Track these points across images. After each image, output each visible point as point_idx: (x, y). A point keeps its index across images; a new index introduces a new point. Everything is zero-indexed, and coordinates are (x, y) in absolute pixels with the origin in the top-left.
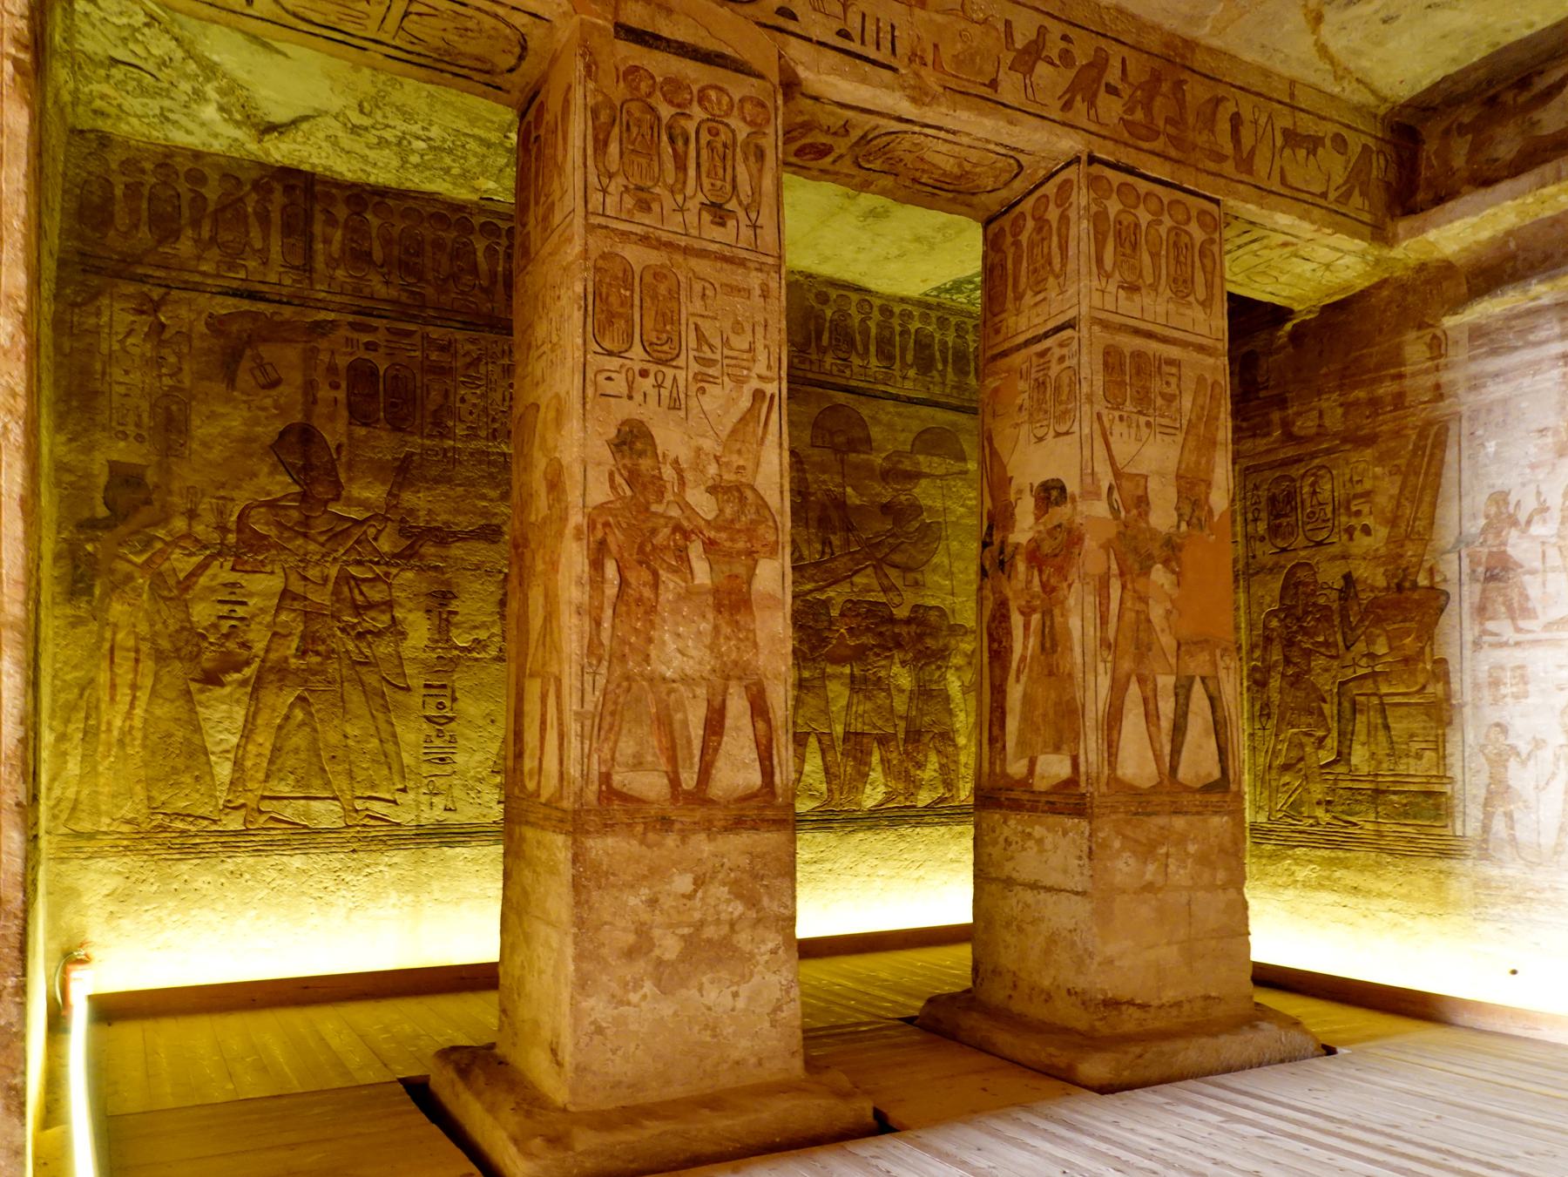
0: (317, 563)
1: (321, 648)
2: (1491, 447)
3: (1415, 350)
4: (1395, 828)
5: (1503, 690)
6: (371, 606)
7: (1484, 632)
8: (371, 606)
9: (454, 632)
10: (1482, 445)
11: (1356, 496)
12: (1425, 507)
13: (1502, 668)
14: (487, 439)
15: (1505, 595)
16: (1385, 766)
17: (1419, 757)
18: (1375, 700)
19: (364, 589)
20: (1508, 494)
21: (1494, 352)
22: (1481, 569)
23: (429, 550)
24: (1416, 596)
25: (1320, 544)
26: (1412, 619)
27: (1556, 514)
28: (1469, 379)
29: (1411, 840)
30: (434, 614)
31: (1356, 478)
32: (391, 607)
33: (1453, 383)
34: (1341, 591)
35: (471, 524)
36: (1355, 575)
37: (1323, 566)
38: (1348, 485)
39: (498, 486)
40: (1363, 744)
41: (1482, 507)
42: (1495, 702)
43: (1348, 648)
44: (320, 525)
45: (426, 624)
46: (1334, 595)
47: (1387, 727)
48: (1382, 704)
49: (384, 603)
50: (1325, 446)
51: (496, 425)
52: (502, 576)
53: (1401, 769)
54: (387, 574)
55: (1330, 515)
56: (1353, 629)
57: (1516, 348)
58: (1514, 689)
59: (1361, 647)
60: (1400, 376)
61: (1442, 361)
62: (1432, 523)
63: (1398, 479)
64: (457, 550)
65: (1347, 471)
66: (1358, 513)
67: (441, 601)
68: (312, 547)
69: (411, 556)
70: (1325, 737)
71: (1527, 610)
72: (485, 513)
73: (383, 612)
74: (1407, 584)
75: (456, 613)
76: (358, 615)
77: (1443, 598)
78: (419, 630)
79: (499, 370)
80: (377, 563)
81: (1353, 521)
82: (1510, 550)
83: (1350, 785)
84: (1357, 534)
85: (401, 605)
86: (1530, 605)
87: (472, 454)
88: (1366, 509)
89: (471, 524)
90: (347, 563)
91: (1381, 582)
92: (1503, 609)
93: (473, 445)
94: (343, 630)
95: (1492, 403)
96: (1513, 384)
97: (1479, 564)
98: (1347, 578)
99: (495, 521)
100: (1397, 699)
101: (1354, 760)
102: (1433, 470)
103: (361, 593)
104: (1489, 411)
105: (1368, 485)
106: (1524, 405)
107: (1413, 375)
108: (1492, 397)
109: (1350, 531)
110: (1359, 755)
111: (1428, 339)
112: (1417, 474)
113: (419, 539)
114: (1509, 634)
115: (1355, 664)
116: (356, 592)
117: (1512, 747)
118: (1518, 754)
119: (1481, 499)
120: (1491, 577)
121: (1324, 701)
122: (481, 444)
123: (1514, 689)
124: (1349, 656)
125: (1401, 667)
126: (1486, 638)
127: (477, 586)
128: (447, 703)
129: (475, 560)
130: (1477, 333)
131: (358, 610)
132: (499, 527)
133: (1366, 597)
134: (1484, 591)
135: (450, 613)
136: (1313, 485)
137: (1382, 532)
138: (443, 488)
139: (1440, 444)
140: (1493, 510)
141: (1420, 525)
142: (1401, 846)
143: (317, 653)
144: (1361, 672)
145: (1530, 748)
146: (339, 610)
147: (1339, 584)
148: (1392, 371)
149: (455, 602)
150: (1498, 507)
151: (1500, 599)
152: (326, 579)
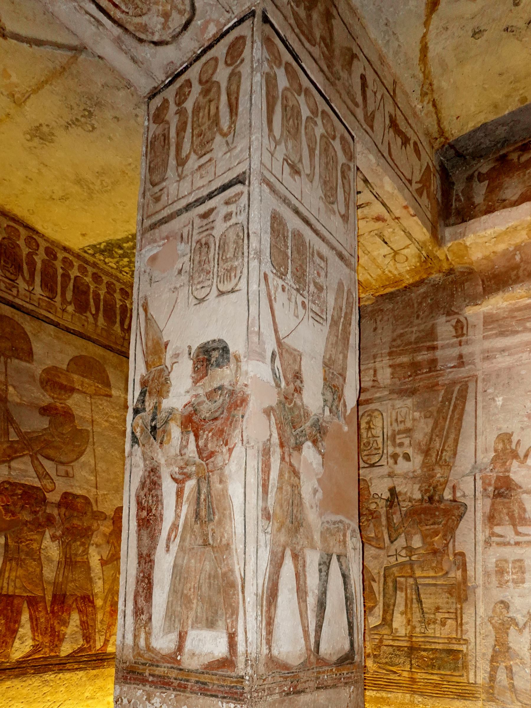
2: (499, 401)
3: (444, 328)
4: (424, 676)
5: (506, 577)
7: (493, 534)
10: (493, 399)
11: (400, 432)
12: (451, 441)
13: (506, 561)
15: (509, 508)
16: (418, 630)
17: (443, 624)
18: (411, 581)
20: (511, 435)
21: (502, 334)
22: (491, 489)
24: (442, 506)
25: (373, 465)
26: (439, 524)
28: (483, 352)
29: (437, 685)
31: (399, 420)
33: (472, 354)
34: (387, 500)
36: (398, 489)
37: (374, 482)
38: (395, 424)
40: (402, 613)
41: (493, 445)
42: (500, 585)
43: (392, 542)
46: (382, 503)
47: (420, 601)
48: (416, 584)
50: (378, 395)
53: (430, 632)
55: (380, 445)
56: (396, 530)
57: (517, 332)
58: (515, 577)
59: (401, 542)
60: (434, 348)
61: (464, 338)
62: (455, 454)
63: (431, 421)
66: (401, 445)
70: (374, 607)
71: (525, 519)
74: (437, 498)
77: (462, 508)
81: (398, 450)
82: (512, 475)
83: (391, 643)
84: (400, 460)
86: (527, 516)
88: (407, 441)
91: (417, 495)
92: (507, 518)
95: (500, 369)
96: (516, 357)
97: (490, 485)
98: (392, 491)
100: (427, 581)
101: (395, 625)
102: (456, 416)
104: (498, 376)
105: (409, 424)
107: (443, 347)
108: (500, 366)
109: (395, 457)
110: (399, 622)
111: (454, 322)
112: (445, 419)
114: (511, 537)
115: (397, 554)
117: (513, 619)
118: (517, 625)
119: (492, 438)
120: (498, 495)
121: (374, 580)
123: (515, 577)
124: (393, 547)
125: (430, 557)
126: (494, 539)
130: (489, 320)
133: (405, 506)
134: (493, 504)
136: (368, 423)
137: (418, 459)
139: (463, 396)
140: (500, 446)
141: (446, 455)
142: (429, 690)
144: (401, 560)
145: (525, 619)
147: (386, 495)
148: (429, 344)
150: (504, 444)
151: (505, 511)
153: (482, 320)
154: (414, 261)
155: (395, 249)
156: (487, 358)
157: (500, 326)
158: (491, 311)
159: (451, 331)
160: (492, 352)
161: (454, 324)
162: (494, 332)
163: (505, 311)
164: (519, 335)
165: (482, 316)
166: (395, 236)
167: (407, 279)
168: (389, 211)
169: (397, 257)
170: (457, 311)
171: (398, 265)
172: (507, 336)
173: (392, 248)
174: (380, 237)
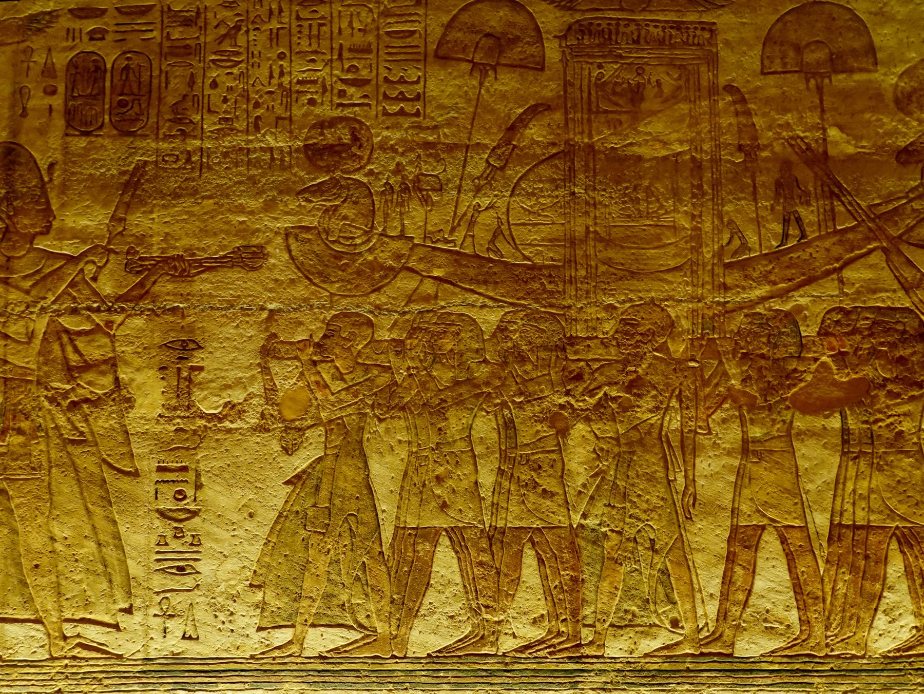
0: (20, 316)
1: (25, 425)
6: (87, 367)
8: (87, 367)
9: (197, 395)
14: (247, 132)
19: (80, 343)
23: (164, 286)
30: (172, 371)
32: (115, 365)
35: (223, 248)
39: (260, 193)
44: (24, 266)
45: (160, 386)
49: (105, 362)
51: (260, 112)
52: (265, 315)
54: (109, 324)
64: (203, 284)
67: (180, 355)
68: (14, 295)
69: (141, 297)
72: (243, 231)
73: (103, 373)
75: (201, 369)
76: (71, 379)
78: (150, 395)
79: (263, 38)
80: (98, 310)
85: (127, 363)
87: (226, 155)
89: (223, 248)
90: (58, 313)
93: (227, 142)
94: (52, 400)
99: (255, 241)
103: (76, 350)
113: (150, 273)
116: (69, 349)
122: (239, 140)
127: (230, 330)
128: (190, 492)
129: (226, 294)
131: (70, 372)
132: (261, 247)
135: (193, 369)
138: (186, 203)
143: (20, 432)
146: (47, 374)
149: (199, 354)
152: (31, 336)
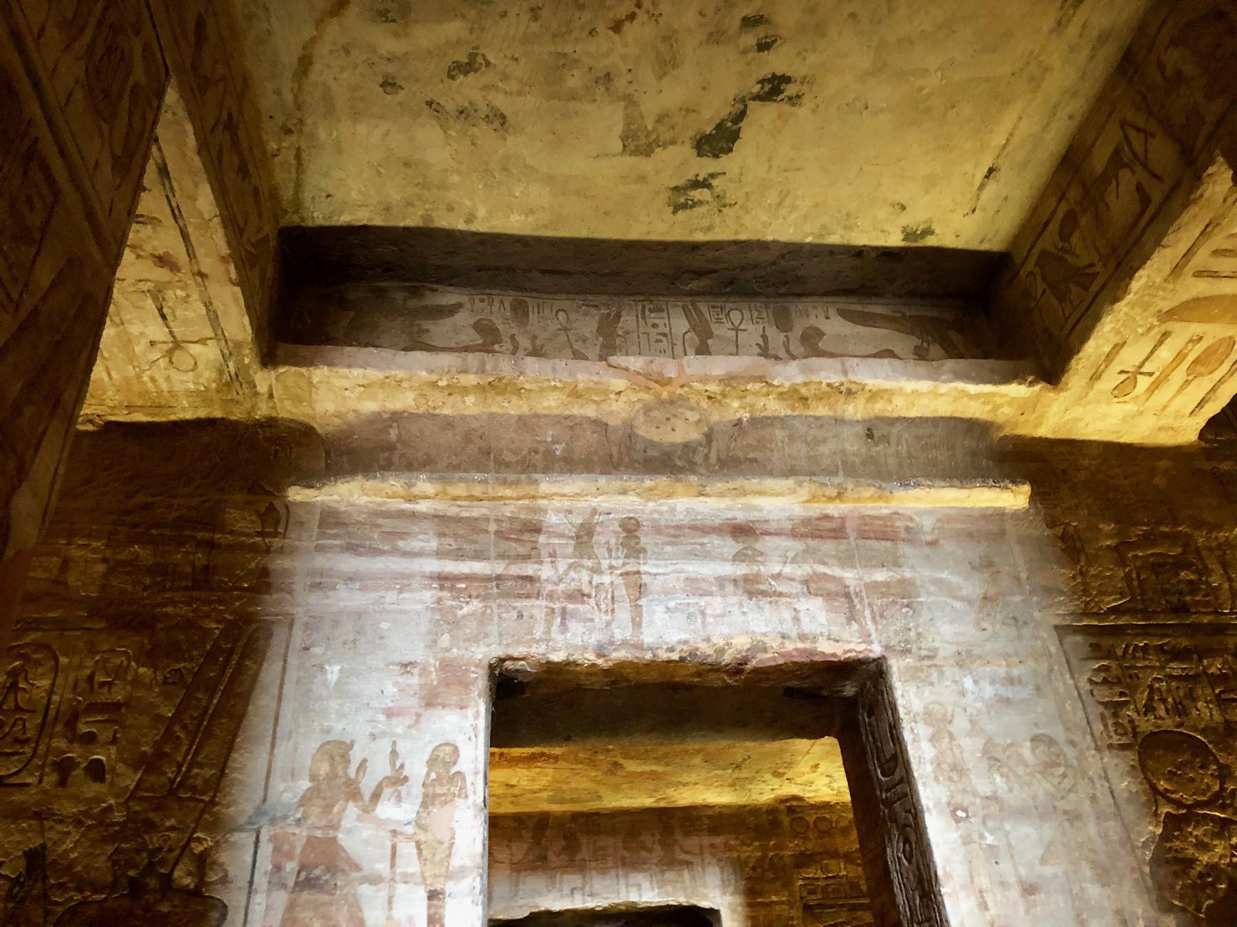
21: (352, 549)
27: (415, 790)
57: (381, 552)
65: (89, 663)
96: (374, 595)
106: (384, 625)
108: (341, 604)
153: (318, 517)
154: (207, 375)
155: (179, 338)
156: (319, 586)
157: (349, 534)
158: (336, 505)
159: (252, 522)
160: (330, 576)
161: (262, 511)
162: (338, 542)
163: (362, 512)
164: (383, 558)
165: (319, 511)
166: (186, 310)
167: (184, 408)
168: (191, 254)
169: (177, 353)
170: (271, 489)
171: (172, 372)
172: (361, 555)
173: (171, 332)
174: (155, 299)
